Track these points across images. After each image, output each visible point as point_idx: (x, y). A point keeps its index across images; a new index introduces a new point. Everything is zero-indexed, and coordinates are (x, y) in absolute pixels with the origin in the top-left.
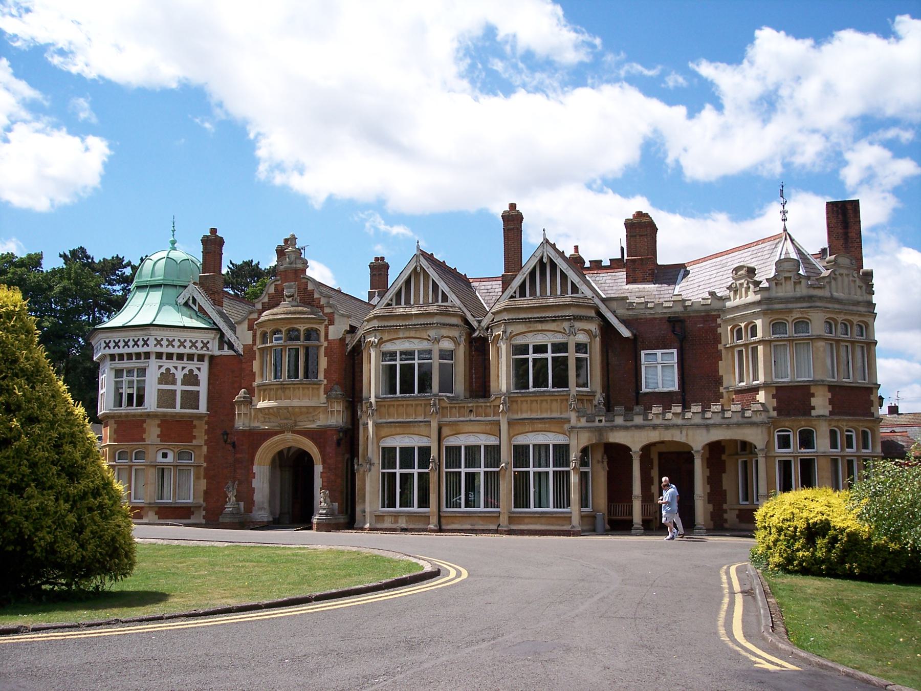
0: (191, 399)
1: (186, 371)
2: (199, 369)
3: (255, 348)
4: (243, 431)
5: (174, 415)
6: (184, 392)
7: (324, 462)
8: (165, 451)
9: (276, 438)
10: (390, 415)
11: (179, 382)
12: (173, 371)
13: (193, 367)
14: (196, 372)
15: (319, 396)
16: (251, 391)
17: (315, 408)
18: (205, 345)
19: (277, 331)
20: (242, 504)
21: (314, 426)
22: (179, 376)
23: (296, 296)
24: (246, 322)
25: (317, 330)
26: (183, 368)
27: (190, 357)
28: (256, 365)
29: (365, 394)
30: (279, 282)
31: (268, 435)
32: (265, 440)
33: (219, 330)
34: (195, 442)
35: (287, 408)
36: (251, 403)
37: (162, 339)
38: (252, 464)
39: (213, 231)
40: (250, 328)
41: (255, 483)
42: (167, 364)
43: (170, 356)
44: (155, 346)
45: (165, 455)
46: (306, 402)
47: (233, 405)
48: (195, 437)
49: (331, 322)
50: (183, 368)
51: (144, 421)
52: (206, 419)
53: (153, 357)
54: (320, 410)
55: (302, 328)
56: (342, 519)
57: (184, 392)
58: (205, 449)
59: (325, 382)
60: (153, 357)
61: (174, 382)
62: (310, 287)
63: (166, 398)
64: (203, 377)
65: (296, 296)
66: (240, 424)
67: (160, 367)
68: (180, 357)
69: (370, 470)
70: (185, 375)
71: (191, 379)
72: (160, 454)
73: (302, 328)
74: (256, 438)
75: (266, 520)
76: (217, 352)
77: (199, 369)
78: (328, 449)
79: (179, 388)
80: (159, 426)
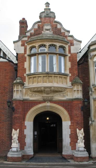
3: (26, 55)
7: (72, 119)
9: (40, 105)
15: (67, 84)
16: (23, 79)
17: (66, 88)
23: (51, 30)
24: (21, 41)
25: (64, 47)
28: (26, 65)
30: (40, 23)
32: (32, 107)
35: (50, 87)
38: (24, 120)
40: (23, 45)
46: (60, 85)
47: (13, 85)
49: (72, 44)
54: (68, 90)
59: (70, 75)
65: (51, 30)
66: (17, 96)
73: (58, 44)
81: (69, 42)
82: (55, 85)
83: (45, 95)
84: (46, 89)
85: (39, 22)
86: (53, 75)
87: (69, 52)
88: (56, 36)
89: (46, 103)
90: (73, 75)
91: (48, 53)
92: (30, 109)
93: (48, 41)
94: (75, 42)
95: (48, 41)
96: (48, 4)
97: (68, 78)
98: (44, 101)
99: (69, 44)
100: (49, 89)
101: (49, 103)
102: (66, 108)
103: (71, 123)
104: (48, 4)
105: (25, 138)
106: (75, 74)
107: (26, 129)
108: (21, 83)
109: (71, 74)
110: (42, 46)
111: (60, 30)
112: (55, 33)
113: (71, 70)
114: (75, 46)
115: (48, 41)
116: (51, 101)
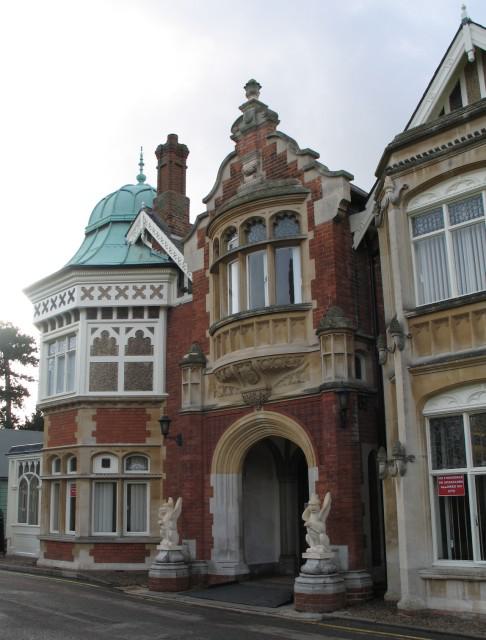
0: (140, 376)
1: (132, 334)
2: (152, 330)
4: (192, 413)
5: (114, 402)
6: (130, 366)
7: (320, 462)
8: (106, 457)
9: (242, 421)
10: (439, 343)
11: (122, 350)
12: (113, 334)
13: (143, 327)
14: (147, 334)
16: (203, 347)
18: (157, 292)
19: (230, 233)
20: (192, 544)
21: (298, 391)
22: (122, 341)
25: (293, 215)
26: (128, 330)
27: (138, 311)
29: (388, 316)
30: (235, 160)
31: (231, 414)
32: (225, 427)
33: (171, 265)
34: (149, 442)
35: (248, 362)
36: (203, 363)
37: (92, 289)
38: (209, 472)
39: (173, 138)
40: (201, 244)
41: (215, 506)
42: (103, 325)
43: (107, 312)
44: (83, 298)
45: (106, 464)
48: (149, 434)
49: (318, 194)
50: (128, 330)
51: (75, 413)
52: (165, 403)
53: (83, 316)
54: (309, 359)
55: (266, 213)
56: (358, 580)
57: (130, 366)
58: (164, 451)
59: (315, 305)
60: (83, 316)
61: (114, 352)
62: (281, 147)
63: (103, 376)
64: (158, 340)
67: (94, 330)
68: (123, 312)
69: (403, 473)
70: (130, 340)
71: (140, 345)
72: (98, 462)
74: (211, 422)
75: (232, 572)
76: (176, 301)
77: (152, 330)
78: (326, 435)
79: (122, 359)
80: (94, 418)
81: (309, 190)
82: (263, 350)
83: (250, 387)
84: (241, 370)
85: (231, 157)
86: (255, 320)
87: (309, 226)
88: (280, 182)
89: (256, 412)
90: (321, 303)
91: (220, 261)
92: (220, 435)
93: (240, 213)
94: (325, 183)
95: (238, 212)
96: (253, 87)
97: (310, 315)
98: (250, 406)
99: (309, 198)
100: (248, 368)
101: (262, 411)
102: (306, 424)
103: (320, 474)
104: (253, 87)
105: (212, 523)
106: (328, 298)
107: (212, 496)
108: (196, 363)
109: (318, 301)
110: (286, 216)
111: (284, 157)
112: (272, 174)
113: (316, 287)
114: (326, 197)
115: (238, 212)
116: (264, 403)
